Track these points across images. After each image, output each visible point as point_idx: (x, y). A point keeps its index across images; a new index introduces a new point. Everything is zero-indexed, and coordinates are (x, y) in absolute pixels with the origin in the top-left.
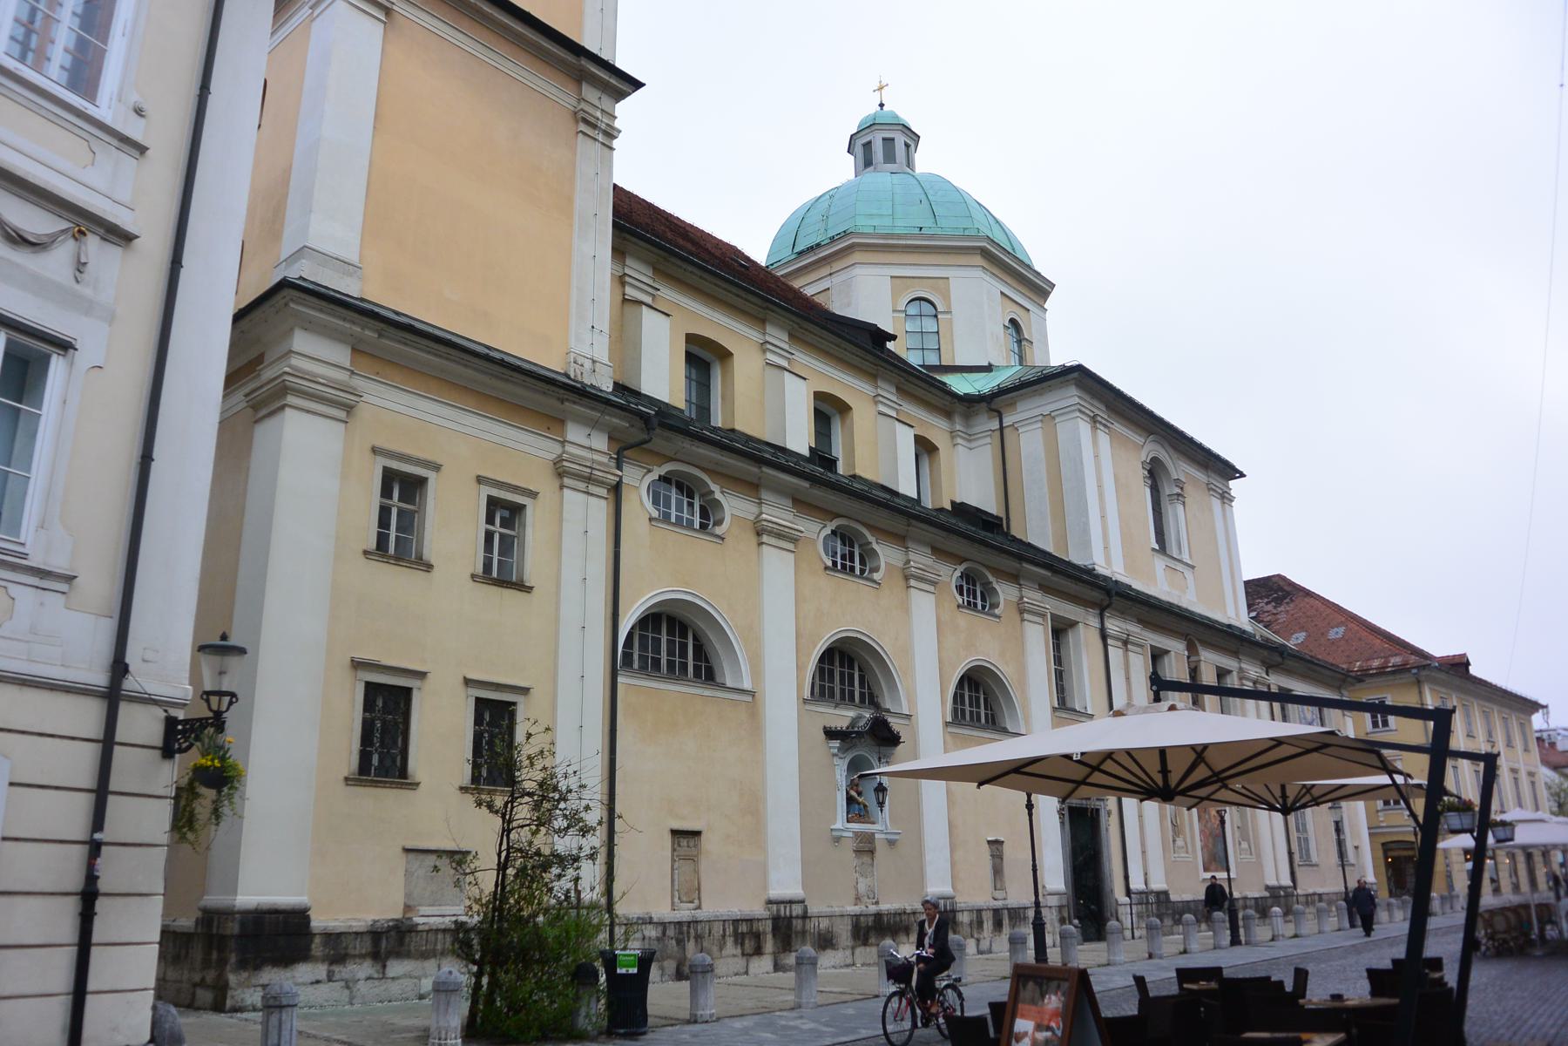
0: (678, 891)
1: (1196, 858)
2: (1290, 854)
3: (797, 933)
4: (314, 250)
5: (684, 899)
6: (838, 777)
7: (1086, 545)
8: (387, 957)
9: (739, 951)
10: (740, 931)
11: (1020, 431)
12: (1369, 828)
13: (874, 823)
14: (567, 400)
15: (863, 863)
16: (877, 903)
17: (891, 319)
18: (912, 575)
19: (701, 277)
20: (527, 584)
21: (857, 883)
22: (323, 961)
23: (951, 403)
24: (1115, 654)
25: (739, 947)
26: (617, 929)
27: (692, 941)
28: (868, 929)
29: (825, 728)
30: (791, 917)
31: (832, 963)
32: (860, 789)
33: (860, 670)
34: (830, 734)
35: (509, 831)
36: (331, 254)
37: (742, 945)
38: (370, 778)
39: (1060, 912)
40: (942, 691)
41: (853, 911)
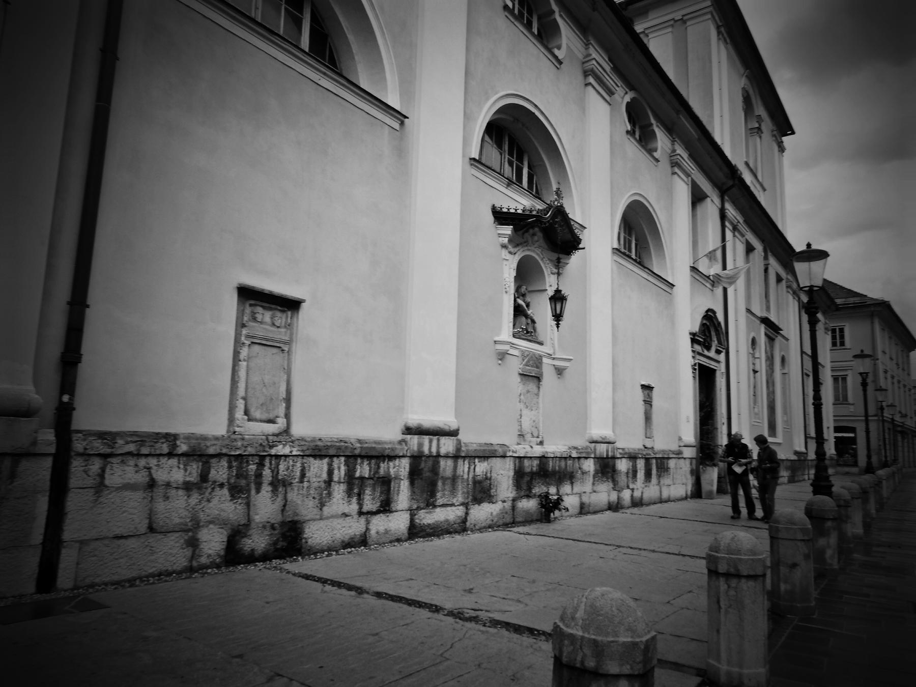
0: (244, 399)
1: (762, 423)
3: (445, 479)
5: (257, 414)
6: (506, 275)
9: (354, 507)
10: (357, 474)
11: (650, 36)
12: (834, 416)
13: (541, 344)
15: (528, 392)
16: (541, 443)
18: (592, 71)
21: (521, 416)
24: (729, 234)
25: (354, 500)
26: (76, 465)
27: (266, 489)
28: (533, 475)
30: (438, 455)
32: (528, 299)
33: (530, 167)
34: (501, 217)
37: (360, 496)
39: (691, 464)
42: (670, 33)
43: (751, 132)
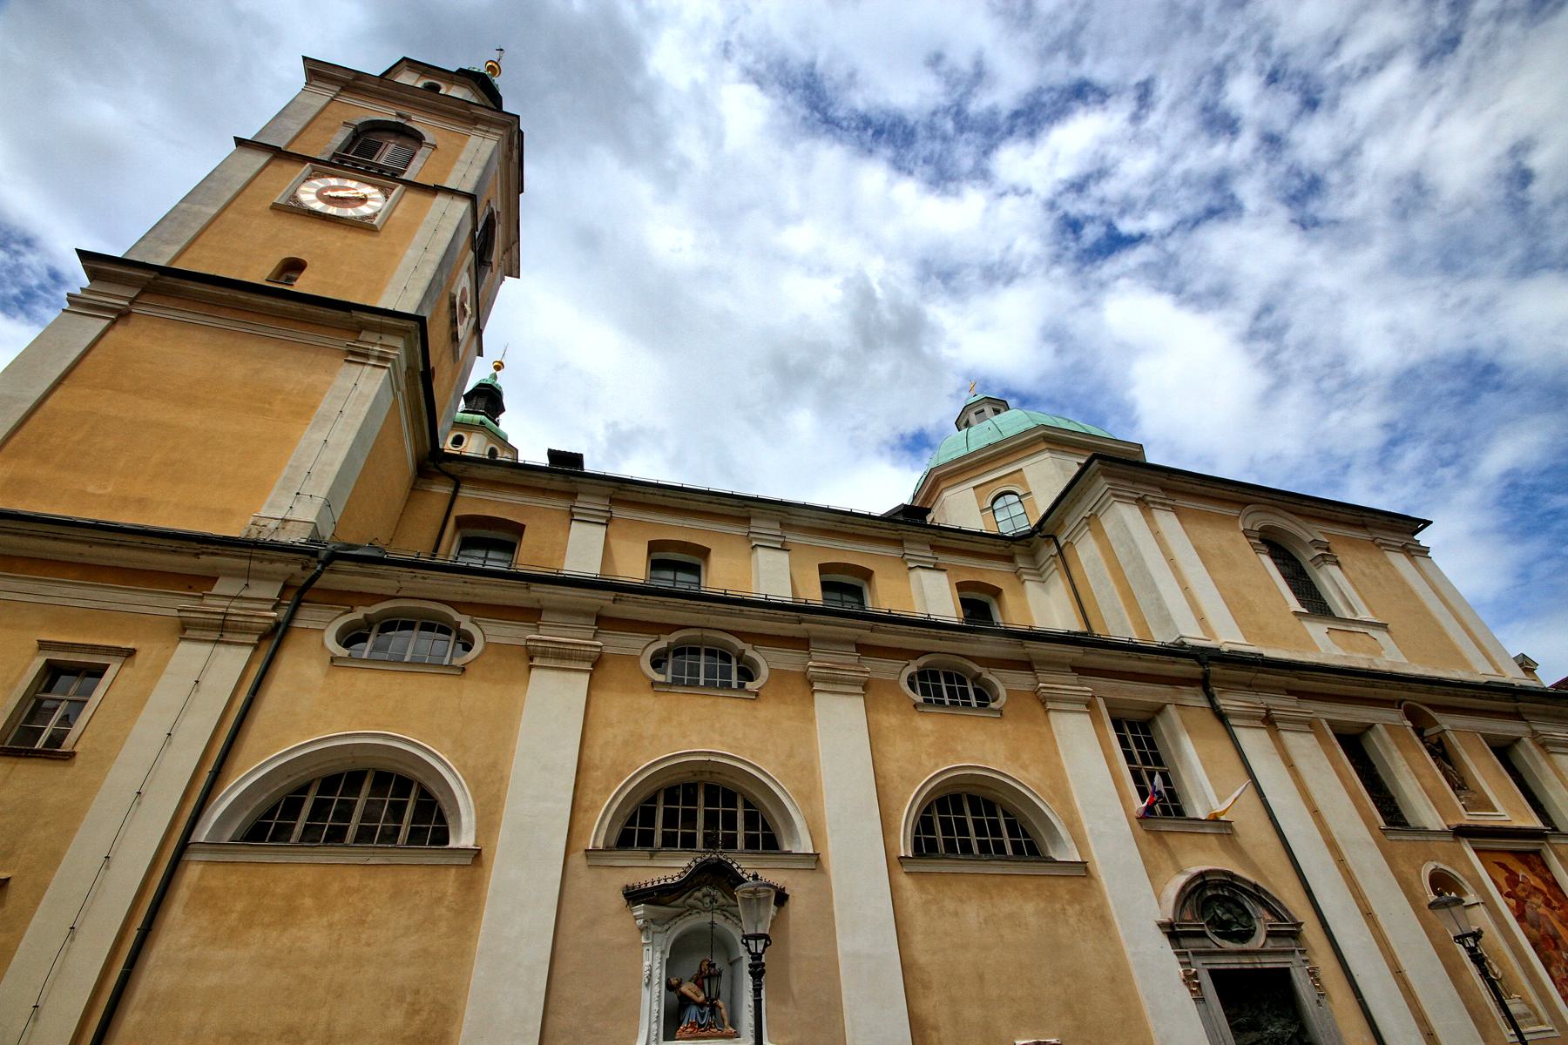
7: (1167, 619)
14: (203, 553)
17: (981, 517)
19: (663, 496)
23: (1006, 547)
34: (634, 896)
42: (1089, 532)
43: (1315, 563)
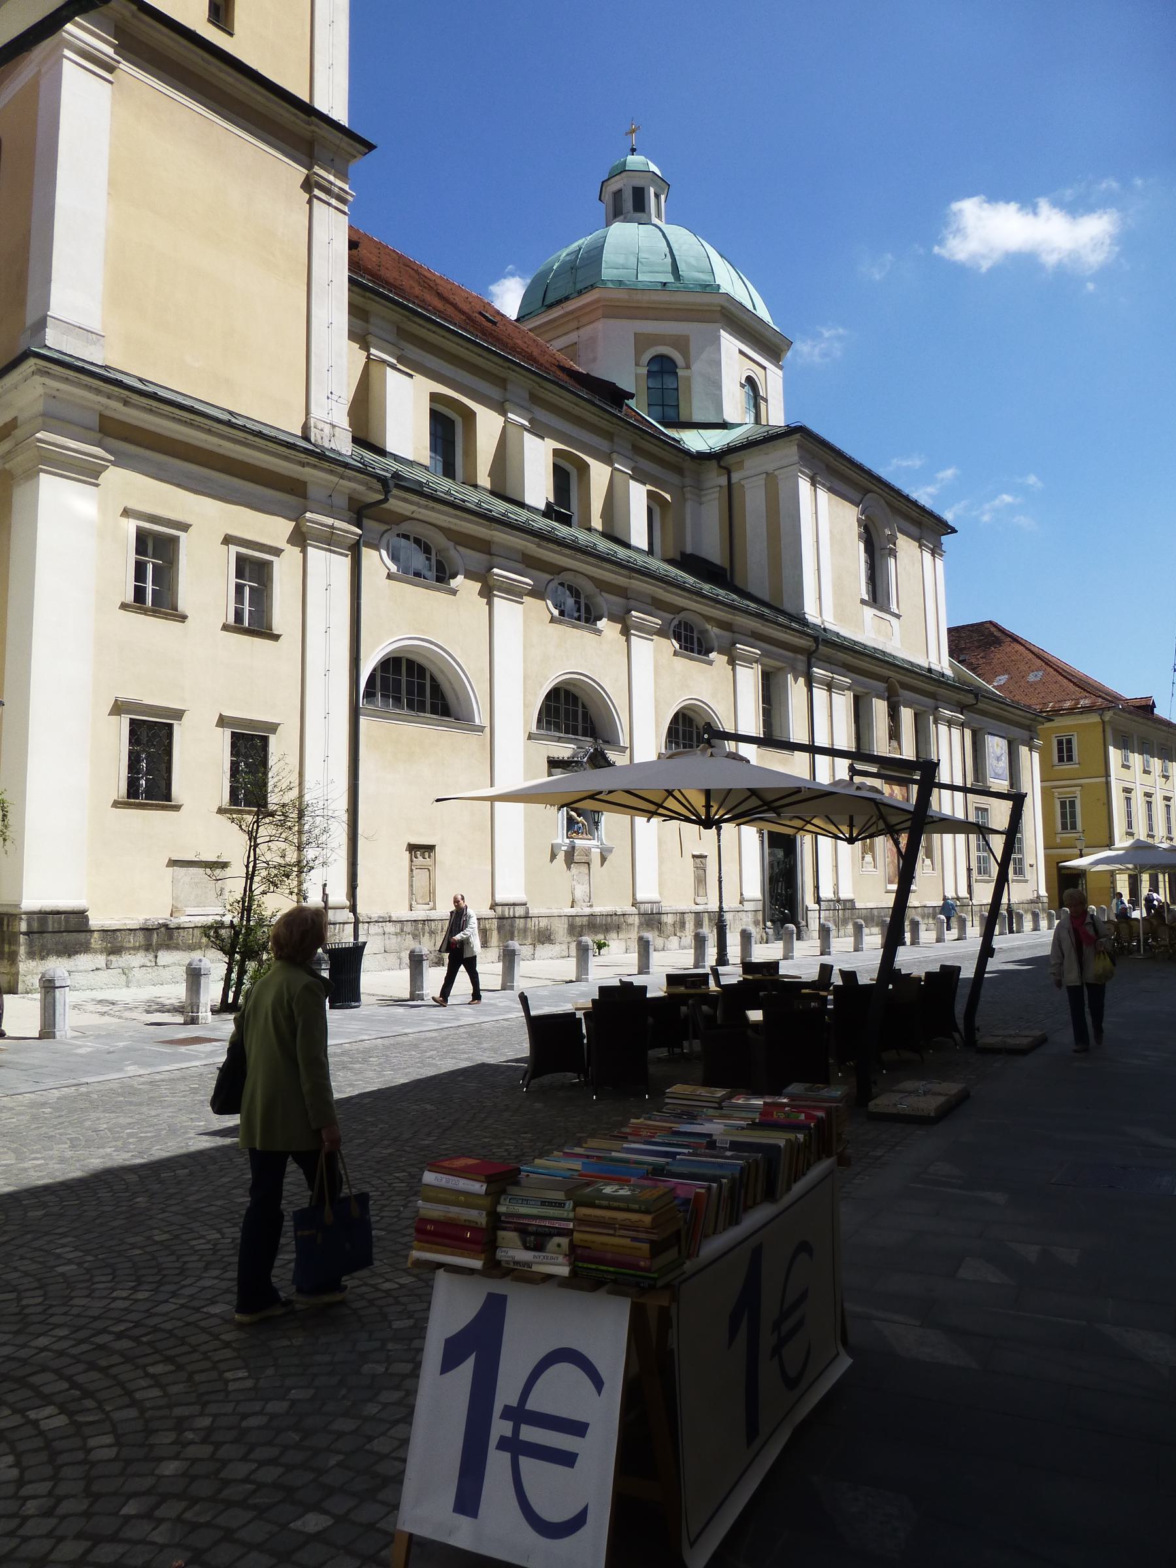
2: (969, 870)
4: (58, 319)
5: (420, 901)
8: (158, 950)
15: (580, 873)
20: (276, 632)
22: (102, 952)
26: (360, 925)
27: (427, 935)
28: (582, 926)
29: (548, 757)
31: (550, 955)
35: (256, 845)
36: (74, 323)
38: (137, 801)
39: (755, 916)
40: (657, 726)
41: (569, 912)
